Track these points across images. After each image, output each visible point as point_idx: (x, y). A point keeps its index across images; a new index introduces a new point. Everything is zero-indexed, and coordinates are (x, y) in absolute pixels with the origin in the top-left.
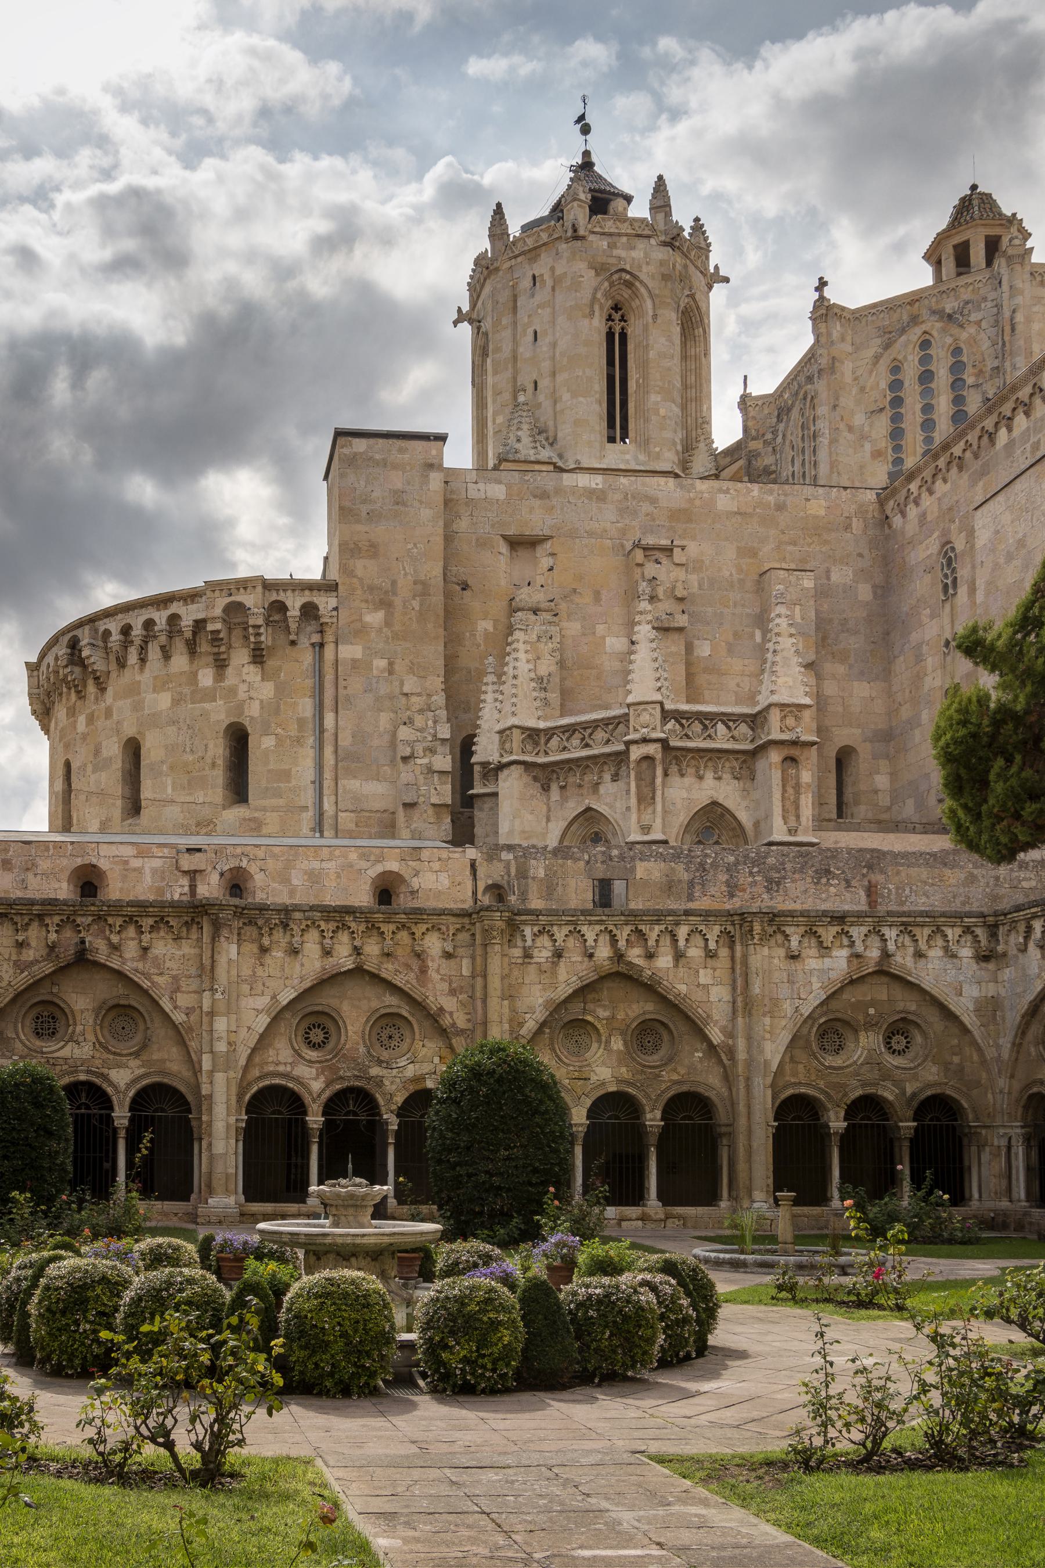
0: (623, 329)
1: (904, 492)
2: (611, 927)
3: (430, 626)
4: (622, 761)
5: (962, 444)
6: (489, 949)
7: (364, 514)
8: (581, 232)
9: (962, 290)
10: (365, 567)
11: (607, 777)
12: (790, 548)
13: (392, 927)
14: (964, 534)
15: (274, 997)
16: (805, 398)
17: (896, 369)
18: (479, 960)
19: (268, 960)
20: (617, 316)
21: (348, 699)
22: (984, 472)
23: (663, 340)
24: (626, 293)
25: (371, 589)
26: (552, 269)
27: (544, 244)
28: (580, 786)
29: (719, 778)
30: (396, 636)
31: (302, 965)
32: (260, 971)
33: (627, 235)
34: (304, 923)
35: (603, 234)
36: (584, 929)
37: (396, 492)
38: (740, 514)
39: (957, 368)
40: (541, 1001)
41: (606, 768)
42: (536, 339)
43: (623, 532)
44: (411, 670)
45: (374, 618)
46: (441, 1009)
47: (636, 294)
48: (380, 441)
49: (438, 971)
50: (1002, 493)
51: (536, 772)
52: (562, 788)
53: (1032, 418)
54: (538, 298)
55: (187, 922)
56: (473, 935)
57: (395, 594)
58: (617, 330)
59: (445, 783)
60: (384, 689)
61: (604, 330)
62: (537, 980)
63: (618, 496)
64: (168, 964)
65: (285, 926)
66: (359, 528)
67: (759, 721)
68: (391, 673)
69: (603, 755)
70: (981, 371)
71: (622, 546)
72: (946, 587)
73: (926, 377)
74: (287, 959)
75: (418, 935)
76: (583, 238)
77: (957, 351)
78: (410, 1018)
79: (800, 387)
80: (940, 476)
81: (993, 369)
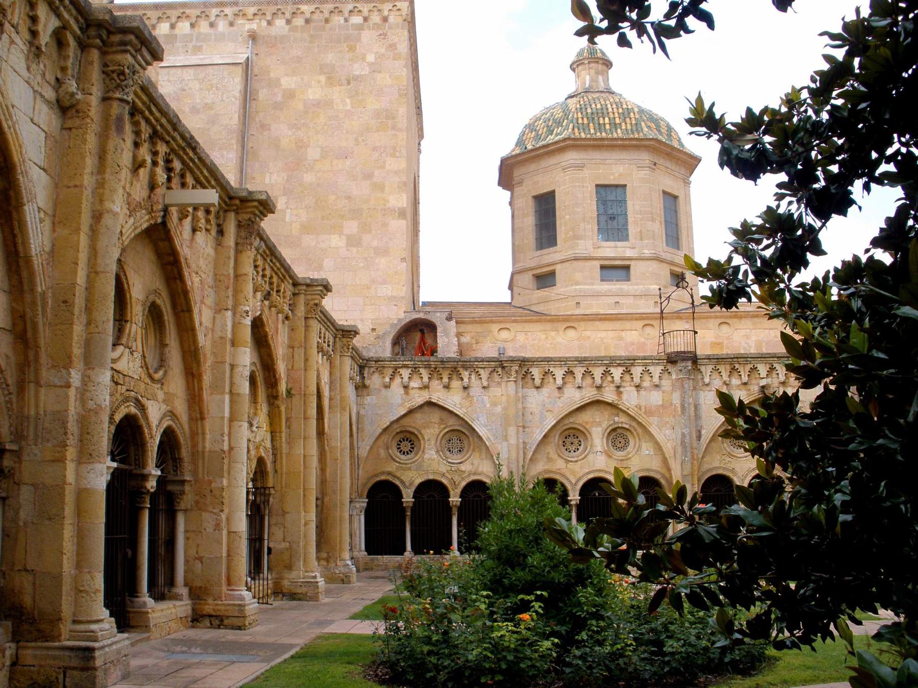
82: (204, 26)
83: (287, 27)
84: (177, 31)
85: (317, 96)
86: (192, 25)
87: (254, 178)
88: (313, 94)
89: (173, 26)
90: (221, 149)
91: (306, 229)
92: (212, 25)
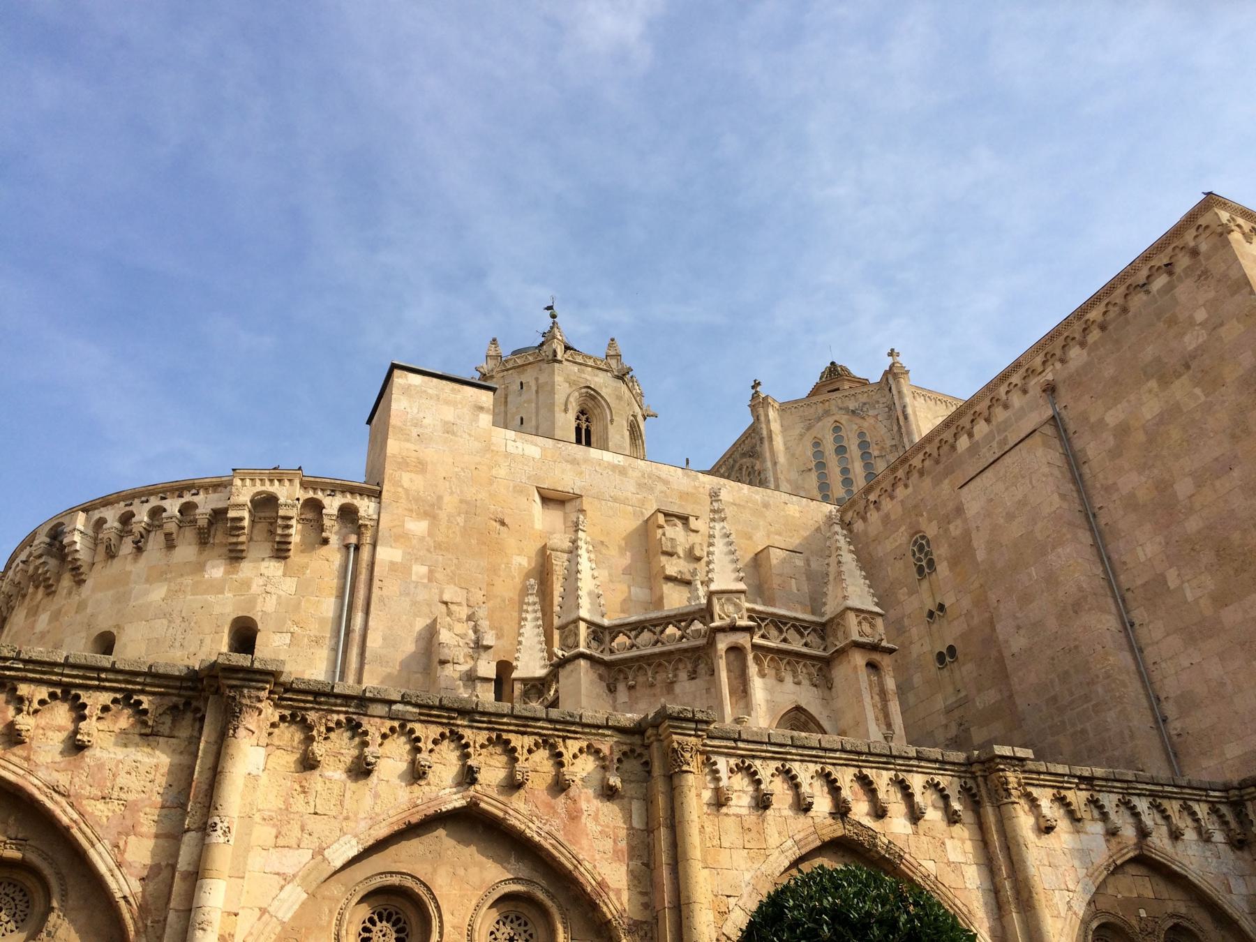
0: (587, 426)
1: (863, 503)
2: (829, 768)
3: (474, 542)
4: (699, 658)
5: (921, 456)
6: (676, 781)
7: (414, 434)
8: (559, 357)
9: (860, 396)
10: (411, 480)
11: (683, 675)
12: (776, 537)
13: (528, 741)
14: (935, 522)
15: (319, 852)
16: (741, 469)
17: (817, 444)
18: (661, 801)
19: (314, 780)
20: (584, 418)
21: (381, 599)
22: (948, 472)
23: (618, 437)
24: (590, 404)
25: (417, 500)
26: (537, 379)
27: (530, 364)
28: (652, 685)
29: (798, 683)
30: (438, 546)
31: (377, 796)
32: (299, 804)
33: (591, 366)
34: (389, 724)
35: (575, 363)
36: (796, 767)
37: (446, 423)
38: (735, 505)
39: (863, 445)
40: (747, 876)
41: (681, 666)
42: (522, 423)
43: (643, 502)
44: (451, 579)
45: (418, 527)
46: (602, 884)
47: (598, 405)
48: (435, 380)
49: (596, 819)
50: (990, 470)
51: (602, 670)
52: (631, 688)
53: (994, 422)
54: (524, 397)
55: (174, 708)
56: (646, 764)
57: (440, 508)
58: (584, 426)
59: (489, 691)
60: (422, 595)
61: (574, 425)
62: (739, 843)
63: (636, 474)
64: (122, 780)
65: (354, 728)
66: (408, 445)
67: (828, 629)
68: (430, 580)
69: (678, 650)
70: (883, 448)
71: (642, 513)
72: (920, 570)
73: (841, 450)
74: (351, 785)
75: (567, 757)
76: (560, 362)
77: (861, 434)
78: (549, 903)
79: (735, 461)
80: (901, 484)
81: (892, 446)
82: (1000, 414)
83: (1085, 352)
84: (977, 436)
85: (1157, 410)
86: (988, 420)
87: (1124, 563)
88: (1150, 408)
89: (971, 435)
90: (1054, 548)
91: (1221, 599)
92: (1006, 407)
